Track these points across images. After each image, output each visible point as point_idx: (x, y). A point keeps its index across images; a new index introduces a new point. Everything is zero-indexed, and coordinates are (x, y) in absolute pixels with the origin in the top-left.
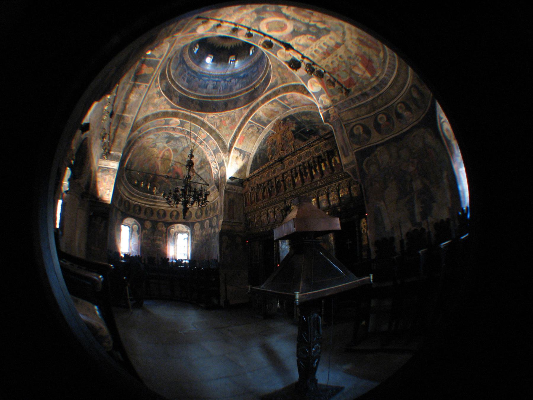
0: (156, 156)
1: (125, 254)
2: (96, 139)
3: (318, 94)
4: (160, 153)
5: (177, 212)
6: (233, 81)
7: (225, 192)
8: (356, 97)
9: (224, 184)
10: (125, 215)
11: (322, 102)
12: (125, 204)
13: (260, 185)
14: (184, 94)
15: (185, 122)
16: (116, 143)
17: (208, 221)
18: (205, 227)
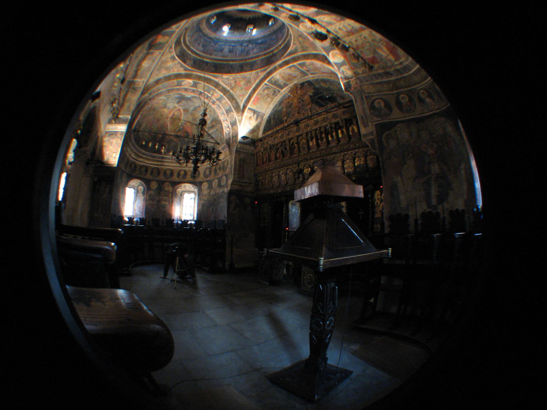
0: (165, 116)
1: (128, 218)
2: (105, 105)
3: (339, 65)
4: (170, 113)
5: (185, 171)
6: (250, 46)
7: (237, 151)
8: (379, 74)
9: (236, 143)
10: (131, 177)
11: (343, 72)
12: (131, 166)
13: (274, 146)
14: (198, 57)
15: (198, 83)
16: (125, 107)
17: (216, 180)
18: (214, 186)
